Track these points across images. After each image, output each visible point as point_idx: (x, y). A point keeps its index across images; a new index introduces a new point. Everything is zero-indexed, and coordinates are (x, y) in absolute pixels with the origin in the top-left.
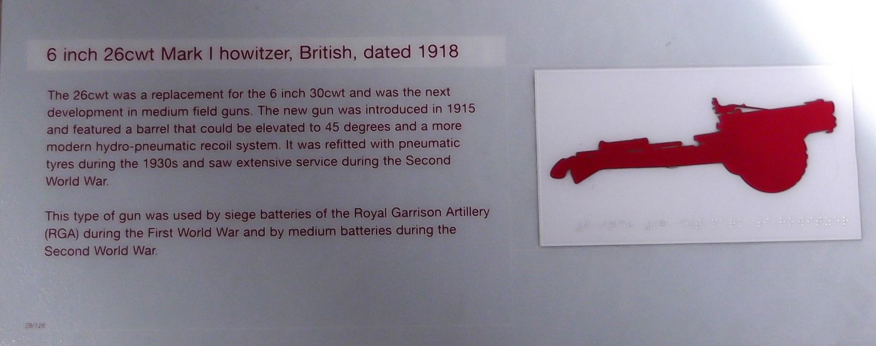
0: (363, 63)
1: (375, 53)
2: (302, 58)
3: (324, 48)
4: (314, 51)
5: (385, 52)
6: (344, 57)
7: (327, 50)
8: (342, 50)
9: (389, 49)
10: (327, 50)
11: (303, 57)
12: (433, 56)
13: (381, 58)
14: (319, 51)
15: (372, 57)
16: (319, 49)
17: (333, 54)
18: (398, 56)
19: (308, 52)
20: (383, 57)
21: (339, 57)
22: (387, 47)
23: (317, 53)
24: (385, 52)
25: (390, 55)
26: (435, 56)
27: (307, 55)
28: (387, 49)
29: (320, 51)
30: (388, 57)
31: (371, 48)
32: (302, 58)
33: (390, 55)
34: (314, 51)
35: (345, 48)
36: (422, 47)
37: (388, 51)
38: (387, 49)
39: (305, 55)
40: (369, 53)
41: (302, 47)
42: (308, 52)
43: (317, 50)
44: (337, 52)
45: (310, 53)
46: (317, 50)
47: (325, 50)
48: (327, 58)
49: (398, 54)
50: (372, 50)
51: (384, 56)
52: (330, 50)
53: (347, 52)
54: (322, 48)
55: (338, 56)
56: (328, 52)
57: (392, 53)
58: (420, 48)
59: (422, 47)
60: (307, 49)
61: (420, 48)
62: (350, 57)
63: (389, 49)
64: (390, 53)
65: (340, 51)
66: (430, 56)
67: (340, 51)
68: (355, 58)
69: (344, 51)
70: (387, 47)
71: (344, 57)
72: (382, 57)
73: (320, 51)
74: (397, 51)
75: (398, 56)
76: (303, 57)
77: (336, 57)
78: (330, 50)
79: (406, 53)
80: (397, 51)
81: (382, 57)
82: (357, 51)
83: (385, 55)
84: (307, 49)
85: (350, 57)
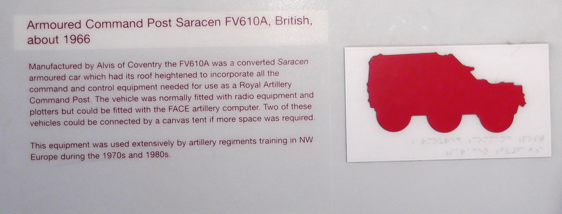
2: (276, 24)
4: (285, 20)
6: (304, 24)
8: (303, 19)
16: (288, 18)
23: (287, 21)
29: (289, 19)
34: (285, 20)
39: (279, 22)
53: (306, 20)
54: (290, 18)
56: (293, 21)
62: (308, 23)
67: (301, 19)
73: (289, 19)
76: (277, 23)
85: (308, 23)
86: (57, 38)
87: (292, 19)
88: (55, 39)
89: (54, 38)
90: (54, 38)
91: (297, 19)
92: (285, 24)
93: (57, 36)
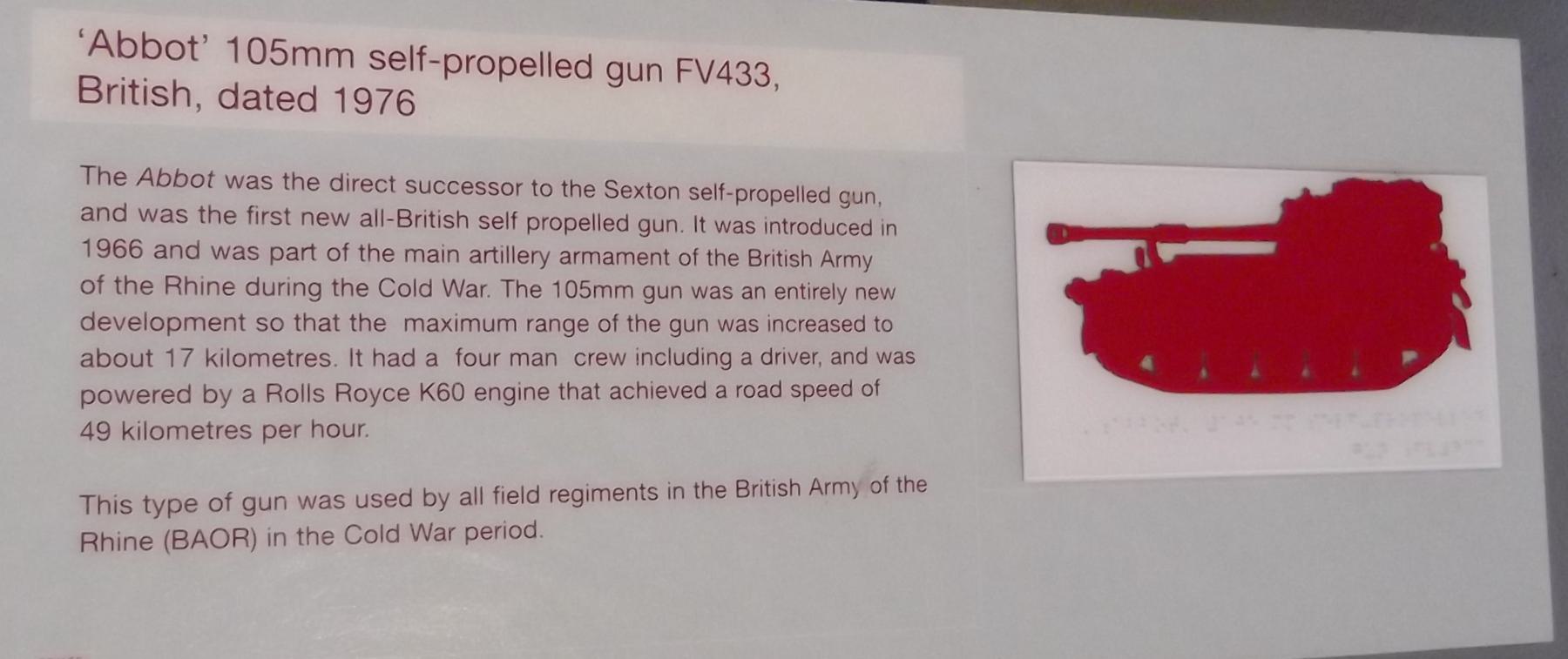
0: (214, 117)
1: (242, 98)
3: (130, 83)
4: (110, 89)
5: (263, 97)
6: (175, 104)
7: (138, 86)
9: (272, 92)
10: (138, 86)
11: (85, 98)
12: (366, 109)
13: (256, 110)
14: (120, 87)
15: (235, 106)
16: (120, 83)
17: (151, 96)
18: (292, 108)
19: (96, 89)
21: (166, 103)
23: (116, 93)
24: (263, 97)
25: (273, 103)
26: (368, 111)
27: (94, 95)
28: (268, 92)
29: (123, 87)
31: (233, 89)
32: (81, 100)
33: (273, 103)
34: (110, 89)
35: (178, 87)
36: (342, 92)
37: (271, 96)
38: (268, 92)
39: (87, 95)
40: (228, 99)
41: (82, 77)
42: (96, 89)
43: (115, 86)
44: (159, 91)
45: (99, 92)
46: (115, 86)
47: (133, 86)
48: (137, 104)
50: (235, 93)
51: (261, 106)
52: (145, 88)
53: (181, 95)
54: (128, 82)
55: (162, 101)
56: (139, 93)
57: (279, 100)
58: (337, 92)
59: (342, 92)
60: (93, 83)
61: (337, 92)
62: (189, 105)
63: (272, 92)
64: (276, 103)
65: (165, 89)
66: (358, 111)
67: (165, 89)
68: (199, 105)
69: (175, 90)
71: (175, 104)
72: (258, 107)
73: (123, 87)
74: (289, 98)
75: (292, 108)
76: (85, 98)
77: (156, 102)
78: (145, 88)
79: (307, 102)
81: (258, 107)
82: (204, 91)
84: (93, 83)
85: (189, 105)
86: (149, 354)
87: (133, 86)
88: (146, 357)
89: (142, 355)
90: (142, 355)
91: (152, 87)
92: (109, 102)
93: (149, 351)
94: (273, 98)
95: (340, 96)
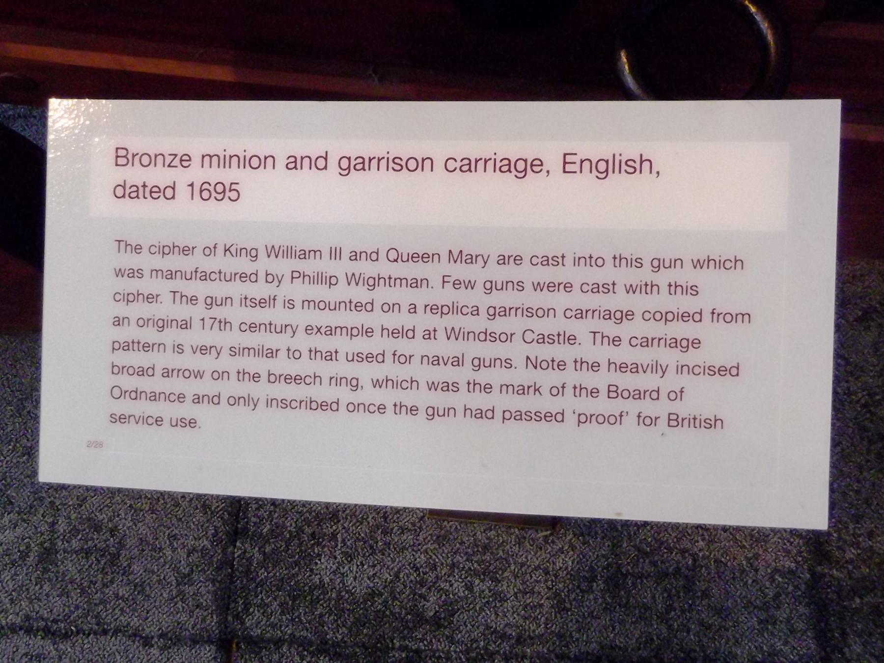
5: (141, 189)
15: (124, 196)
18: (159, 197)
20: (138, 198)
22: (144, 182)
24: (141, 189)
28: (144, 186)
30: (145, 198)
36: (192, 185)
37: (146, 188)
38: (144, 186)
49: (159, 194)
58: (189, 185)
59: (192, 185)
61: (189, 185)
70: (144, 182)
74: (158, 190)
75: (159, 197)
80: (158, 190)
83: (141, 195)
94: (148, 190)
95: (190, 187)
